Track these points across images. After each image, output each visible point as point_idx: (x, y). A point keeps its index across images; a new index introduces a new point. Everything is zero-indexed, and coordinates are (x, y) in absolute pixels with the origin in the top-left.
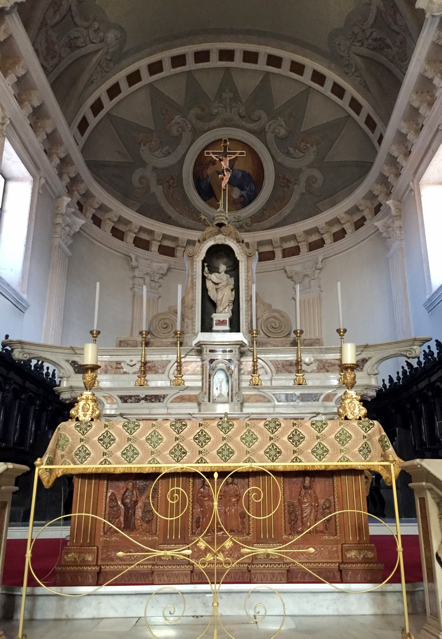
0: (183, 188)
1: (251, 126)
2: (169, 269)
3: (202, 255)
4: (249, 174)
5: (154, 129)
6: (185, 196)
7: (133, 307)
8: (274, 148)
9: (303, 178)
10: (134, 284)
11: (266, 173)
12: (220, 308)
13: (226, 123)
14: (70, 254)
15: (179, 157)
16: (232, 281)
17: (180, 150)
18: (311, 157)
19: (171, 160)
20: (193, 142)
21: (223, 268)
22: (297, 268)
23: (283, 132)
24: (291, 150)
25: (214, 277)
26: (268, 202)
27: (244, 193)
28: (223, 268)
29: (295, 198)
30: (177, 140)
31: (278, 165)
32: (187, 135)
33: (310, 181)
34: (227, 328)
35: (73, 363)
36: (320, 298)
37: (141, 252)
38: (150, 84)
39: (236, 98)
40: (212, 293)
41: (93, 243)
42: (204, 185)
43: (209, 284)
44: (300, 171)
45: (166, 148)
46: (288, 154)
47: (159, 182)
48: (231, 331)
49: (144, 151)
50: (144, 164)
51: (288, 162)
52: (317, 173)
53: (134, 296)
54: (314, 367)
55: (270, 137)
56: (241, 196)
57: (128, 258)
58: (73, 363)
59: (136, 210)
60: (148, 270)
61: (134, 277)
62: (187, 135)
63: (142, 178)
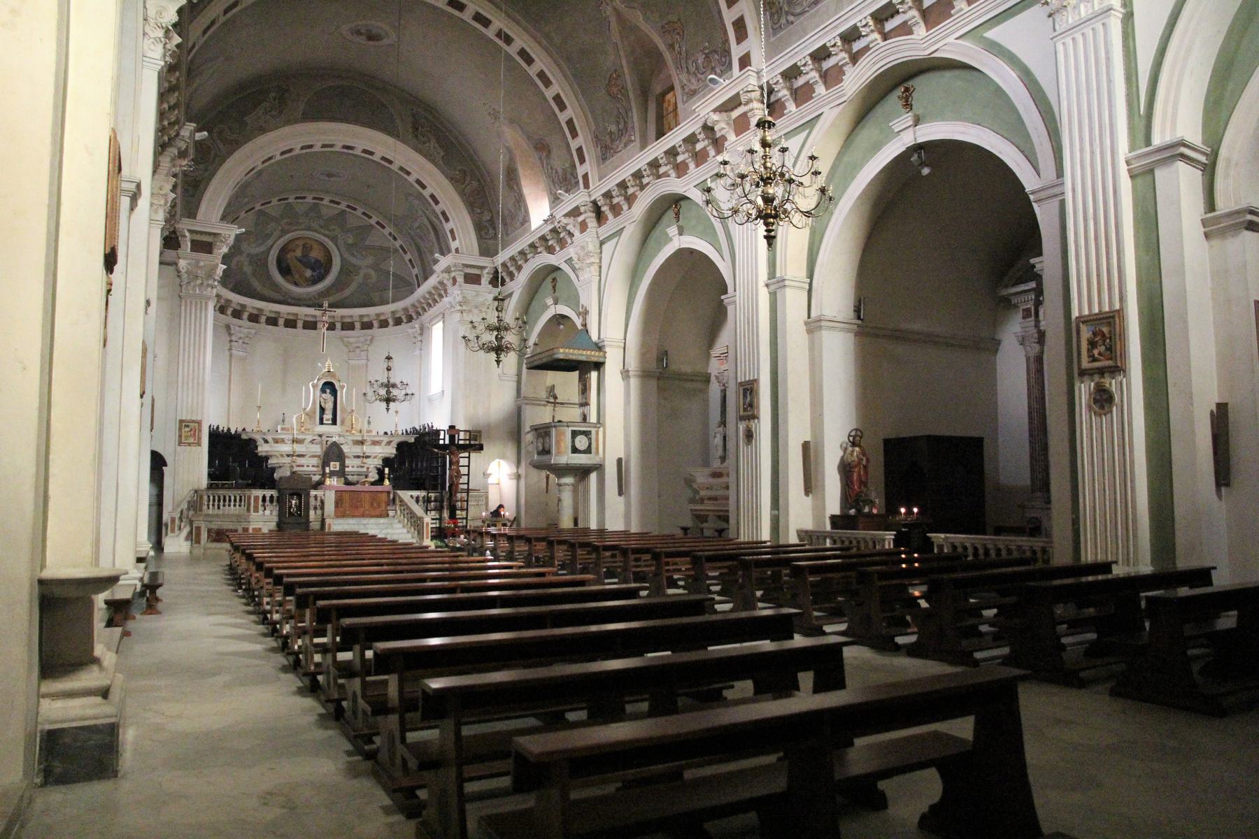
0: (267, 267)
1: (327, 232)
2: (255, 334)
7: (230, 364)
8: (342, 249)
10: (231, 346)
11: (334, 263)
12: (327, 412)
13: (309, 229)
15: (268, 246)
16: (332, 398)
17: (270, 242)
18: (370, 260)
19: (263, 248)
21: (328, 391)
22: (351, 340)
23: (350, 241)
24: (355, 253)
25: (324, 395)
29: (353, 286)
30: (268, 236)
31: (343, 259)
32: (276, 234)
33: (367, 277)
34: (330, 422)
35: (264, 439)
37: (236, 321)
42: (284, 265)
44: (360, 268)
45: (260, 241)
46: (353, 254)
47: (251, 263)
51: (353, 260)
52: (373, 273)
53: (231, 355)
54: (369, 443)
55: (340, 242)
56: (312, 276)
57: (228, 327)
58: (264, 439)
59: (231, 286)
61: (231, 341)
62: (276, 234)
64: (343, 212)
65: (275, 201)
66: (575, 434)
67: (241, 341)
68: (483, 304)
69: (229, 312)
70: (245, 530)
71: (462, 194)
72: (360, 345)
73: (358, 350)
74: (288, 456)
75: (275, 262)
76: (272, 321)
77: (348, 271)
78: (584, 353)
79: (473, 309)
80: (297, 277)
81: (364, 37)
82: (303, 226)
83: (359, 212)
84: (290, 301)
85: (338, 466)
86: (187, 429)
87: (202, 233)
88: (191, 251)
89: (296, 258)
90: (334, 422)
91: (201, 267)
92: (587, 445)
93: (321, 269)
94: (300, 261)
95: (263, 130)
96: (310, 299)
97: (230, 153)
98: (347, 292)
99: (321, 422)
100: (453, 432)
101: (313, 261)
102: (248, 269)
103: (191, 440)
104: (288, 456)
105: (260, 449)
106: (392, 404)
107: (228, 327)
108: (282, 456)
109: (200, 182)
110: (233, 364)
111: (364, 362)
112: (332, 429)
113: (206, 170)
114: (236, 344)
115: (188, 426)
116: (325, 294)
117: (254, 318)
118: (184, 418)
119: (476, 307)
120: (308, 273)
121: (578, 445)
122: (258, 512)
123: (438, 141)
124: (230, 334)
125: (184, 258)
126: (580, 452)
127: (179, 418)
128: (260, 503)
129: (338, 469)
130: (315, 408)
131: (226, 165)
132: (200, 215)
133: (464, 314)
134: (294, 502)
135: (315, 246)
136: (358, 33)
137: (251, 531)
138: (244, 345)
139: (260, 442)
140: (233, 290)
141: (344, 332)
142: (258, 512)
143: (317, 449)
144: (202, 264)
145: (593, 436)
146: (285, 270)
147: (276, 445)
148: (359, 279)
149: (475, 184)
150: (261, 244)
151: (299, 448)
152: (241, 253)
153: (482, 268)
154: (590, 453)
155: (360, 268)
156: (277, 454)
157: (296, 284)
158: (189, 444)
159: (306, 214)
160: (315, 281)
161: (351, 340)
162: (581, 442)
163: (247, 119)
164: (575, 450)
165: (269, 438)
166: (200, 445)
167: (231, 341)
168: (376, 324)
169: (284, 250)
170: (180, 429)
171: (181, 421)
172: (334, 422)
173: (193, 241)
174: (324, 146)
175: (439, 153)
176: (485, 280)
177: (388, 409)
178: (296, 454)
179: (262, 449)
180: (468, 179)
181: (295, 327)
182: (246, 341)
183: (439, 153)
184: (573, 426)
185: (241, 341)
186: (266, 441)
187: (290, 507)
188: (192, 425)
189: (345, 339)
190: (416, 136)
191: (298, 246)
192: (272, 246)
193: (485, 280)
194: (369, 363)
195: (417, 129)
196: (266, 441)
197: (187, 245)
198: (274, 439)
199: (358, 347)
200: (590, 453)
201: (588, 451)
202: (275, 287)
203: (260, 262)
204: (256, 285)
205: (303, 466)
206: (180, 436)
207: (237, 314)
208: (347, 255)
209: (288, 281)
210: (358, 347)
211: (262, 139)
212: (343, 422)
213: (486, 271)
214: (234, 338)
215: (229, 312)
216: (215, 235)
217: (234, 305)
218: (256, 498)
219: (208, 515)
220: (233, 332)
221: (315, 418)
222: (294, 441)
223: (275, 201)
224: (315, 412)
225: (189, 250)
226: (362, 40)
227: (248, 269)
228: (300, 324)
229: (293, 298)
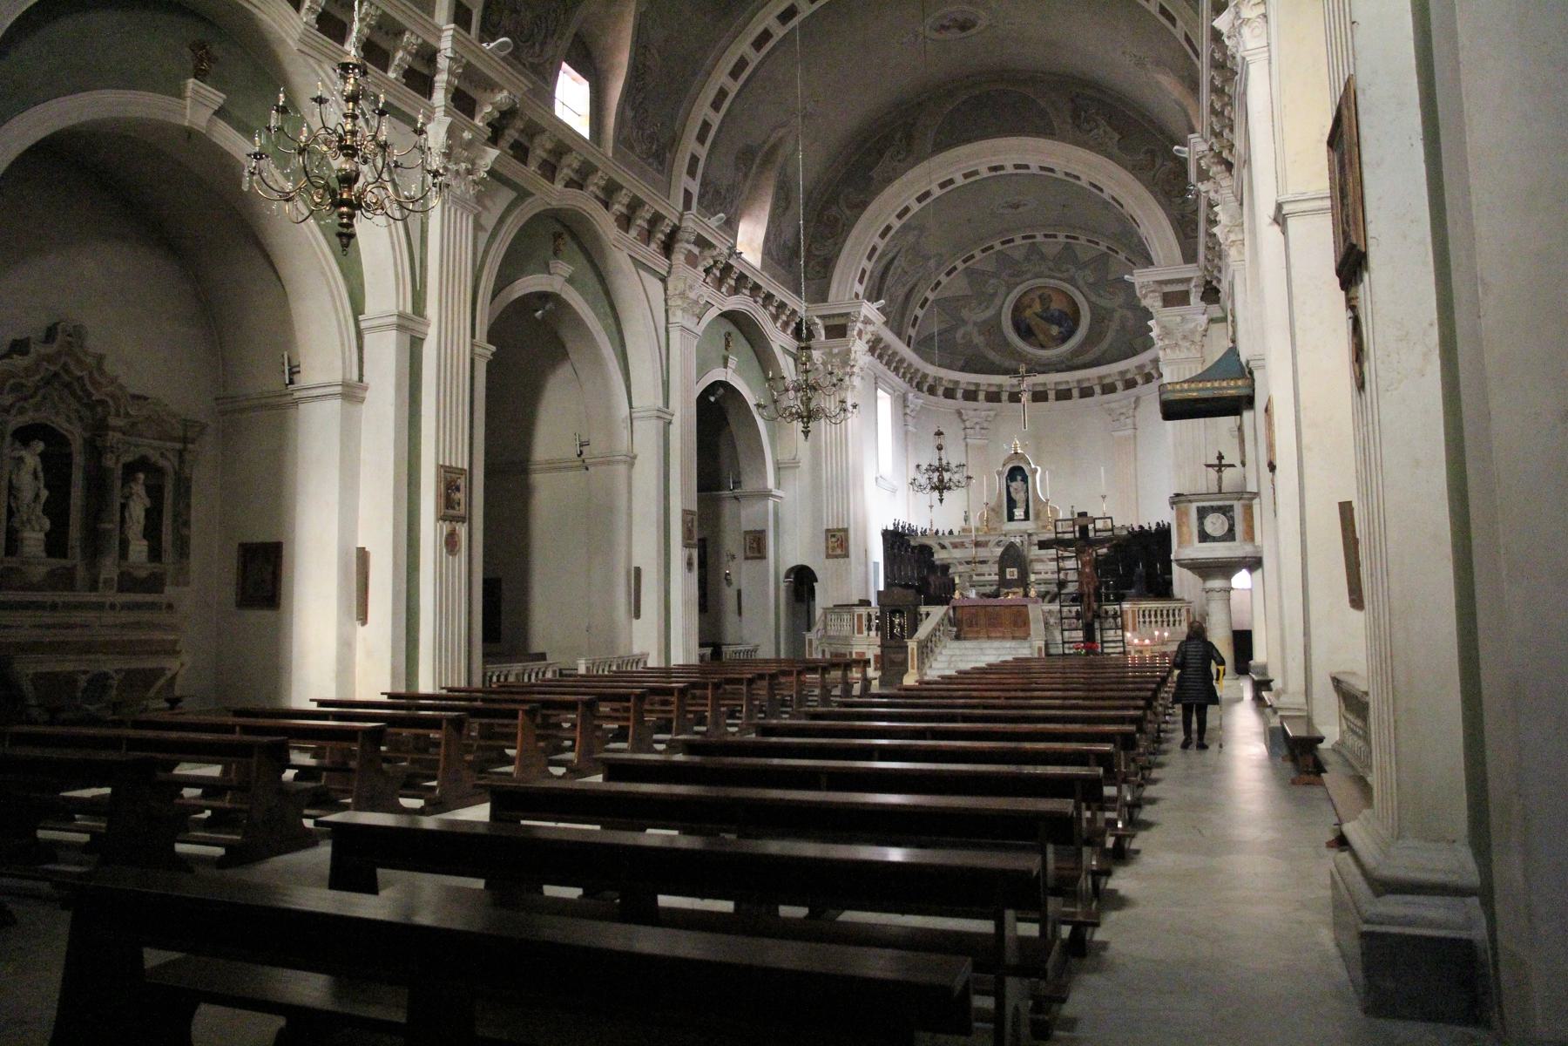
3: (1006, 474)
4: (1066, 314)
5: (970, 294)
6: (1005, 339)
8: (1085, 289)
9: (1117, 315)
11: (1082, 313)
12: (1018, 505)
13: (1037, 276)
14: (914, 430)
17: (997, 302)
19: (990, 313)
20: (1008, 294)
21: (1019, 478)
22: (1113, 405)
23: (1091, 280)
25: (1014, 484)
26: (1087, 338)
27: (1062, 329)
28: (1019, 478)
29: (1110, 336)
35: (940, 544)
36: (1135, 436)
38: (966, 268)
39: (1043, 257)
40: (1013, 495)
41: (930, 410)
43: (1012, 490)
44: (1114, 310)
47: (981, 333)
48: (1024, 520)
49: (965, 313)
50: (964, 322)
51: (1103, 303)
52: (1129, 314)
53: (967, 445)
55: (1081, 283)
56: (1061, 333)
57: (959, 413)
58: (940, 544)
59: (961, 363)
60: (978, 420)
61: (965, 428)
62: (1003, 289)
63: (963, 338)
64: (1067, 247)
65: (978, 255)
66: (1202, 513)
67: (978, 427)
68: (1193, 332)
69: (959, 394)
70: (851, 653)
71: (1151, 185)
72: (1124, 410)
73: (1122, 418)
74: (968, 563)
75: (1010, 322)
76: (1086, 393)
77: (1099, 318)
78: (1209, 385)
79: (1180, 343)
80: (1041, 337)
81: (956, 30)
82: (1065, 275)
83: (1083, 240)
84: (1037, 368)
85: (1016, 573)
86: (834, 540)
87: (833, 316)
88: (826, 338)
89: (1036, 314)
90: (1027, 518)
91: (836, 354)
92: (1226, 527)
93: (1069, 321)
94: (1041, 317)
95: (889, 181)
96: (1063, 362)
97: (857, 218)
98: (1105, 345)
99: (1011, 518)
100: (1083, 521)
101: (1057, 314)
102: (978, 340)
103: (839, 551)
104: (968, 563)
105: (936, 556)
106: (946, 493)
107: (959, 413)
108: (961, 563)
109: (831, 260)
110: (970, 455)
111: (1130, 432)
112: (1029, 526)
113: (836, 244)
114: (972, 431)
115: (833, 536)
116: (1076, 353)
117: (993, 397)
118: (830, 527)
119: (1185, 338)
120: (1055, 330)
121: (1209, 529)
122: (862, 633)
123: (1110, 124)
124: (964, 421)
125: (819, 349)
126: (1214, 539)
127: (825, 527)
128: (865, 622)
129: (1016, 577)
130: (1002, 501)
131: (854, 232)
132: (832, 297)
133: (1168, 351)
134: (897, 621)
135: (1054, 297)
136: (943, 28)
137: (854, 656)
138: (983, 431)
139: (936, 548)
140: (962, 370)
141: (1106, 397)
142: (862, 633)
143: (999, 551)
144: (836, 351)
145: (1238, 513)
146: (1025, 331)
147: (955, 550)
148: (1114, 326)
149: (1170, 164)
150: (987, 308)
151: (983, 553)
152: (964, 322)
153: (1188, 280)
154: (1233, 539)
155: (1114, 310)
156: (954, 561)
157: (1043, 347)
158: (837, 557)
159: (1027, 259)
160: (1064, 339)
161: (1113, 405)
162: (1215, 524)
163: (873, 174)
164: (1204, 537)
165: (946, 542)
166: (847, 555)
167: (965, 428)
168: (1140, 380)
169: (1018, 309)
170: (827, 539)
171: (828, 531)
172: (1027, 518)
173: (826, 328)
174: (966, 176)
175: (1111, 139)
176: (1195, 299)
177: (941, 500)
178: (977, 560)
179: (940, 556)
180: (1159, 161)
181: (999, 401)
182: (985, 425)
183: (1111, 139)
184: (1196, 501)
185: (978, 427)
186: (943, 547)
187: (892, 627)
188: (838, 534)
189: (1106, 406)
190: (1078, 126)
191: (1033, 300)
192: (1001, 307)
193: (1195, 299)
194: (1138, 432)
195: (1079, 117)
196: (943, 547)
197: (821, 333)
198: (952, 544)
199: (1122, 414)
200: (1233, 539)
201: (1230, 535)
202: (1019, 356)
203: (991, 328)
204: (992, 355)
205: (984, 575)
206: (827, 548)
207: (971, 395)
208: (1093, 298)
209: (1031, 344)
210: (1122, 414)
211: (889, 191)
212: (1037, 516)
213: (1193, 284)
214: (968, 424)
215: (959, 394)
216: (847, 314)
217: (963, 386)
218: (860, 616)
219: (829, 637)
220: (965, 417)
221: (1002, 514)
222: (977, 544)
223: (978, 255)
224: (1001, 506)
225: (823, 338)
226: (954, 34)
227: (978, 340)
228: (1052, 395)
229: (1040, 365)
